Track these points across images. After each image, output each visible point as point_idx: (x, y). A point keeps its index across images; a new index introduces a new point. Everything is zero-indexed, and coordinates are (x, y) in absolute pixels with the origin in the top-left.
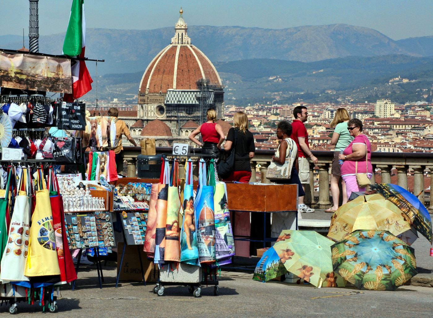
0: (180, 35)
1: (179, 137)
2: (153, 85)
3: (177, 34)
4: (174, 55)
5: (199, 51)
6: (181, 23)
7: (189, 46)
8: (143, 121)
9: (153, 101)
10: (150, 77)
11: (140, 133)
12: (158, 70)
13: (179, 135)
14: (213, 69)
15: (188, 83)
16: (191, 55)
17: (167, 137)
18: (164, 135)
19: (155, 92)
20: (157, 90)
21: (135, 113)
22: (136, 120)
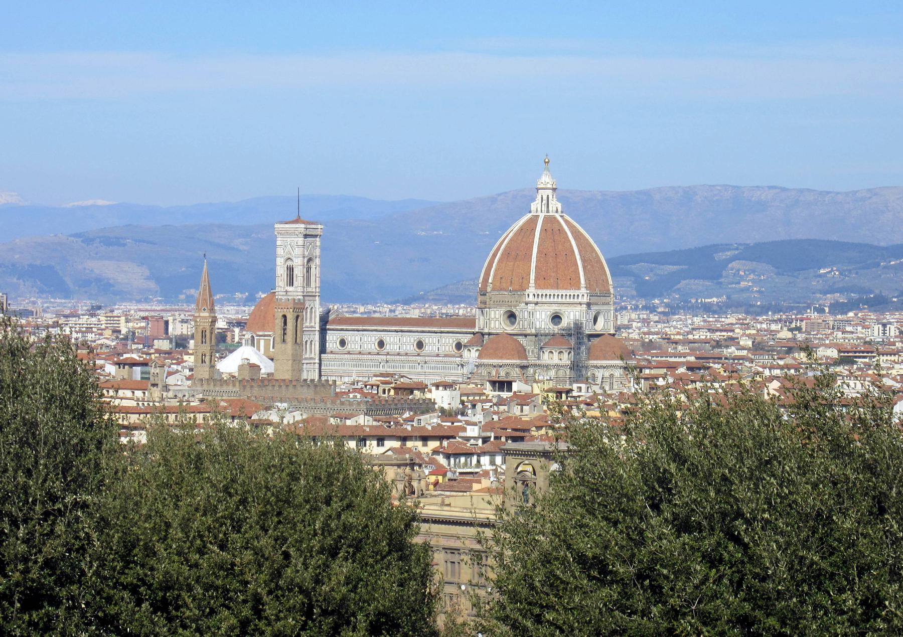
0: (545, 198)
1: (538, 362)
2: (499, 277)
3: (539, 197)
4: (534, 230)
5: (575, 223)
6: (546, 180)
7: (558, 216)
8: (483, 335)
9: (498, 304)
10: (494, 265)
11: (477, 354)
12: (507, 254)
13: (539, 358)
14: (596, 253)
15: (553, 274)
16: (561, 230)
17: (518, 362)
18: (514, 359)
19: (501, 290)
20: (504, 285)
21: (471, 322)
22: (474, 333)
